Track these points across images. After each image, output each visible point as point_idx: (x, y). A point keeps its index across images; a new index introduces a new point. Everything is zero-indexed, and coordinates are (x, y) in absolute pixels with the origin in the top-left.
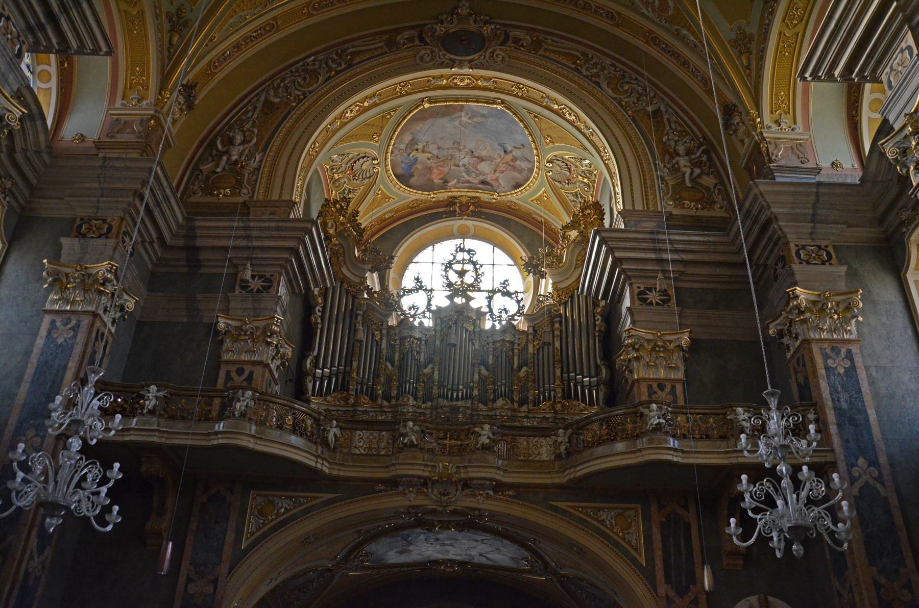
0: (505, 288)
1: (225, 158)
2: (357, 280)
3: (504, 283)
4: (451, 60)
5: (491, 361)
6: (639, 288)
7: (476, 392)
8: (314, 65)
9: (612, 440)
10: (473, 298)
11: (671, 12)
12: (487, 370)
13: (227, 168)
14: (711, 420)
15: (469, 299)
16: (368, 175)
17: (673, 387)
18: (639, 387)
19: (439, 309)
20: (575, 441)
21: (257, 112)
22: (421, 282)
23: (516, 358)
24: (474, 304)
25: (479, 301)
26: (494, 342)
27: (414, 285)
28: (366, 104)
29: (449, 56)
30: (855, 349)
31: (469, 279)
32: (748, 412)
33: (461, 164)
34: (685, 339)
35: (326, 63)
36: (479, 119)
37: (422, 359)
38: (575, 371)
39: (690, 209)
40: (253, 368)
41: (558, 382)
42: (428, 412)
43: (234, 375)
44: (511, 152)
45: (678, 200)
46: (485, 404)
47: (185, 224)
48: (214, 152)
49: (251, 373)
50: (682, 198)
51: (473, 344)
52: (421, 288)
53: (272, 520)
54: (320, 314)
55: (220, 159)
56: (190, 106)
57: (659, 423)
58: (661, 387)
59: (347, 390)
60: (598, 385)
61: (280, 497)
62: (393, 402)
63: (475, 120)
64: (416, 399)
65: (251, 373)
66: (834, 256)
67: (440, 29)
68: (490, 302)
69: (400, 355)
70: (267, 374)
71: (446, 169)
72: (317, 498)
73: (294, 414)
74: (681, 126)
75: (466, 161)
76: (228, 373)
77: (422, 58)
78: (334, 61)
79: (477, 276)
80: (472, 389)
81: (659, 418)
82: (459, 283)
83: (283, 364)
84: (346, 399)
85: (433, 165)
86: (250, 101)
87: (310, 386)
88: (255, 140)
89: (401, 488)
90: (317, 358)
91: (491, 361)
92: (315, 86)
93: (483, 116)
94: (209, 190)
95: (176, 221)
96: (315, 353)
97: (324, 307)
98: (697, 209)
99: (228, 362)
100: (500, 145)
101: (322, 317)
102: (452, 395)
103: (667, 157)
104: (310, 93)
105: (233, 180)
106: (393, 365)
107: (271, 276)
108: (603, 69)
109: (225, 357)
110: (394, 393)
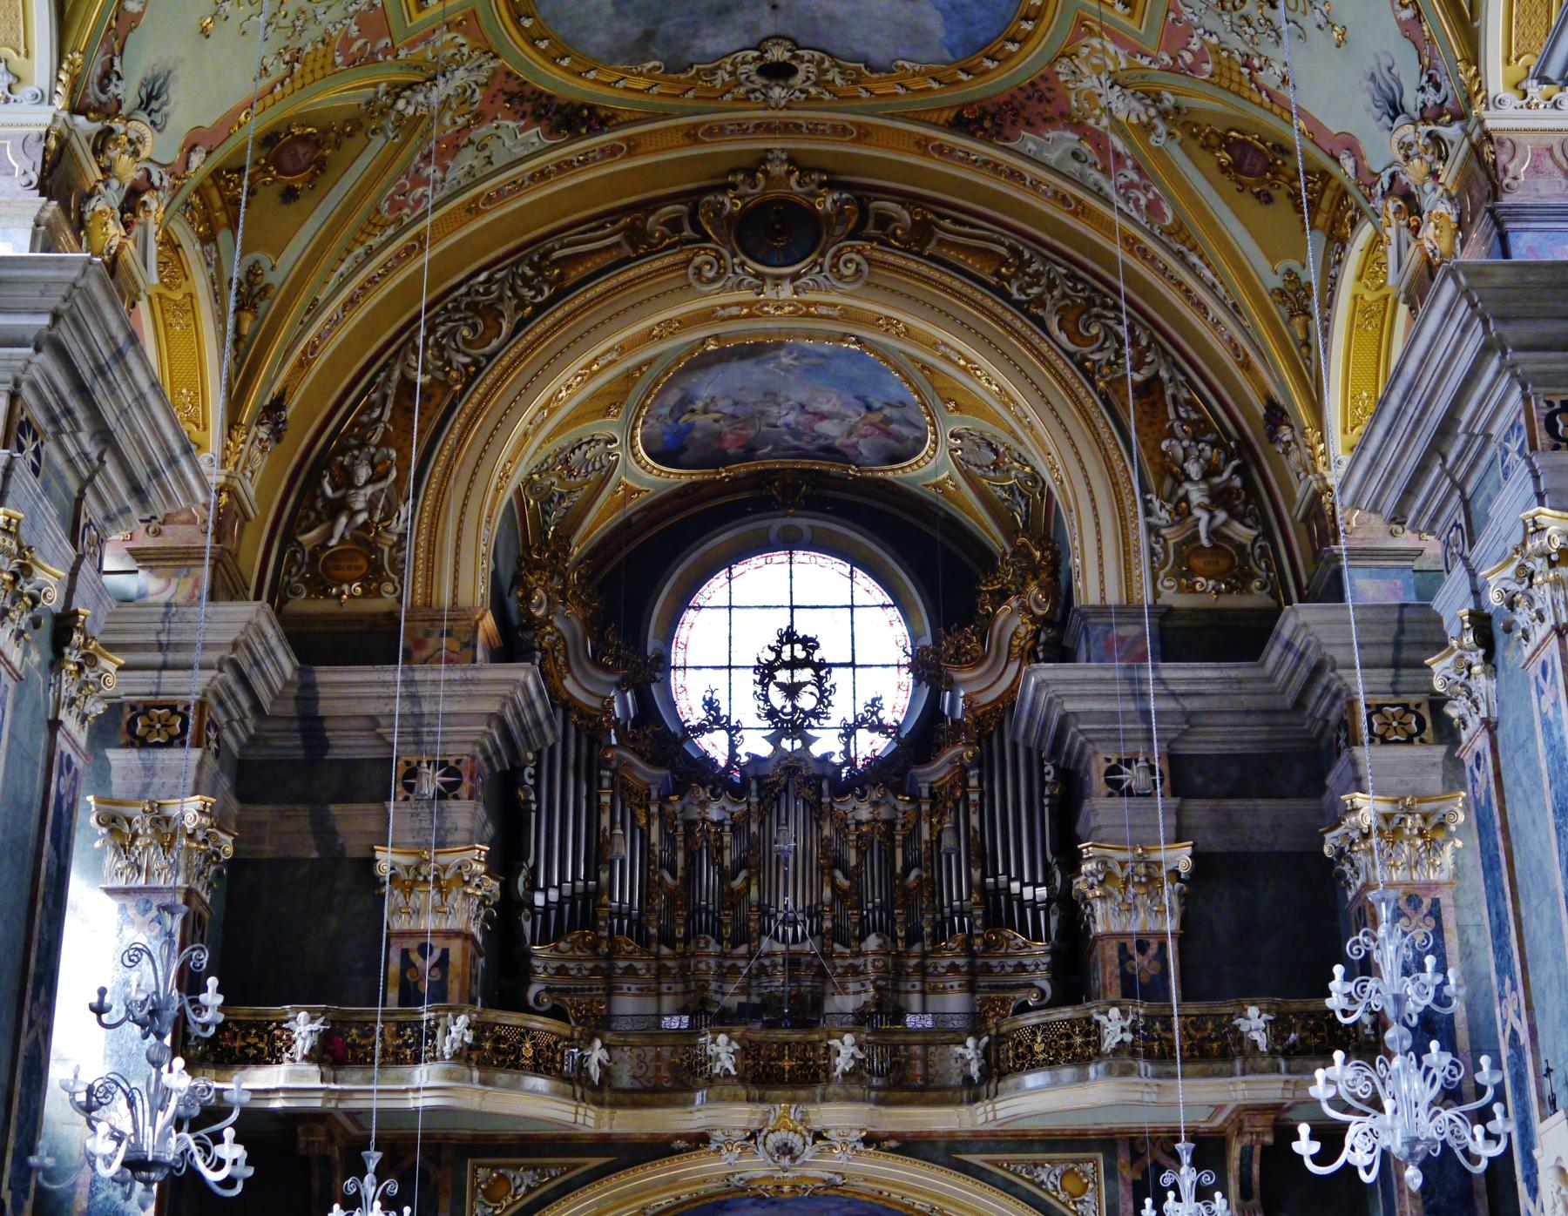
0: (874, 713)
1: (343, 520)
2: (596, 703)
3: (873, 705)
4: (757, 275)
5: (853, 862)
6: (1108, 760)
7: (827, 924)
8: (487, 292)
9: (1051, 1063)
10: (815, 739)
11: (1169, 222)
12: (846, 876)
13: (347, 536)
14: (1210, 1025)
15: (808, 741)
16: (597, 465)
17: (1163, 947)
18: (1103, 947)
19: (755, 759)
20: (993, 1055)
21: (389, 405)
22: (717, 710)
23: (899, 852)
24: (816, 750)
25: (826, 743)
26: (859, 823)
27: (703, 715)
28: (595, 367)
29: (753, 266)
30: (1446, 900)
31: (807, 701)
32: (1268, 1012)
33: (779, 423)
34: (1181, 857)
35: (513, 288)
36: (815, 360)
37: (727, 862)
38: (1007, 871)
39: (1206, 593)
40: (446, 944)
41: (976, 897)
42: (741, 963)
43: (415, 957)
44: (880, 409)
45: (1185, 574)
46: (847, 945)
47: (296, 677)
48: (319, 504)
49: (445, 952)
50: (1191, 573)
51: (820, 828)
52: (717, 719)
53: (508, 1207)
54: (531, 782)
55: (334, 518)
56: (277, 435)
57: (1122, 1041)
58: (1142, 946)
59: (595, 928)
60: (1048, 901)
61: (517, 1167)
62: (680, 947)
63: (806, 361)
64: (720, 942)
65: (445, 952)
66: (1429, 724)
67: (730, 203)
68: (847, 744)
69: (686, 855)
70: (469, 945)
71: (751, 433)
72: (577, 1166)
73: (533, 1038)
74: (1197, 409)
75: (791, 418)
76: (405, 954)
77: (699, 269)
78: (527, 282)
79: (822, 692)
80: (819, 915)
81: (1123, 1030)
82: (788, 709)
83: (488, 918)
84: (594, 946)
85: (726, 429)
86: (371, 382)
87: (527, 926)
88: (394, 474)
89: (713, 1146)
90: (534, 871)
91: (853, 862)
92: (495, 343)
93: (822, 356)
94: (320, 586)
95: (282, 674)
96: (531, 862)
97: (538, 768)
98: (1218, 592)
99: (403, 935)
100: (857, 397)
101: (537, 788)
102: (785, 932)
103: (1168, 483)
104: (490, 357)
105: (362, 562)
106: (674, 875)
107: (458, 762)
108: (1051, 286)
109: (400, 923)
110: (680, 932)
